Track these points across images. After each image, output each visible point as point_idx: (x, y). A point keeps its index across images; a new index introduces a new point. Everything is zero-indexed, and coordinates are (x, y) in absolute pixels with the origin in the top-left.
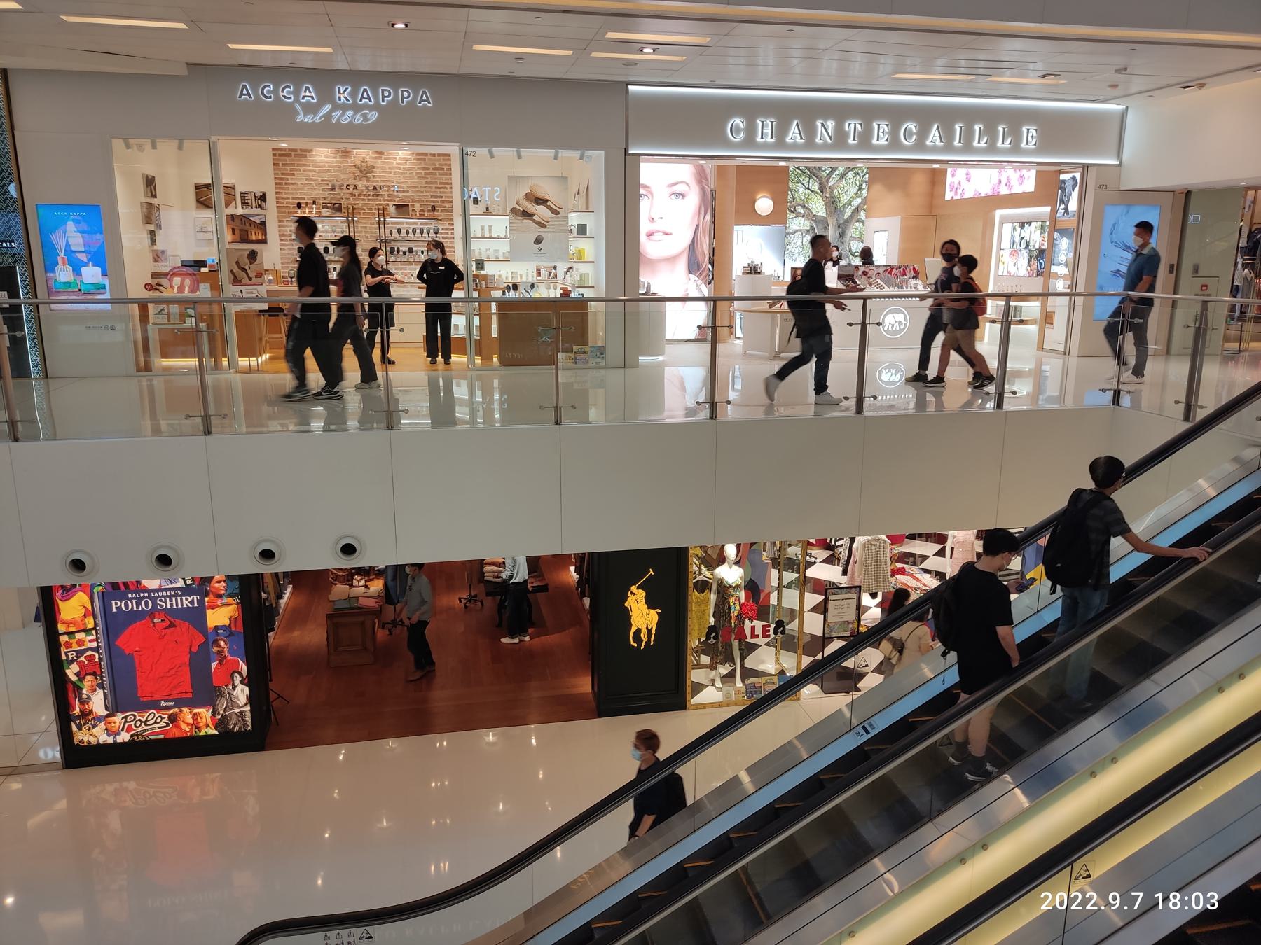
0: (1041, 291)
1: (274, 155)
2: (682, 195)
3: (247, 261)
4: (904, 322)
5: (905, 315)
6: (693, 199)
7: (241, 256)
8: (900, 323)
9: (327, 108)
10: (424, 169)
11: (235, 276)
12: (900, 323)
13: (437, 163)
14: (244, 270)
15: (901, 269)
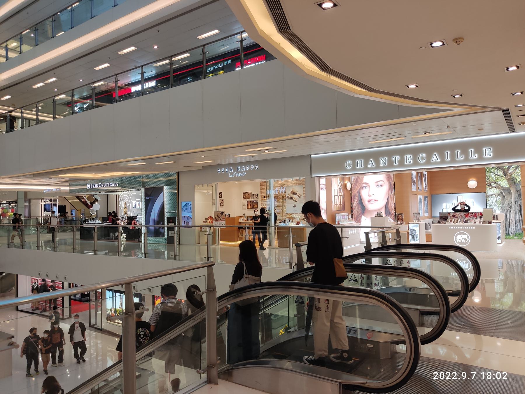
0: (370, 226)
1: (261, 183)
2: (382, 186)
3: (220, 215)
4: (467, 239)
5: (467, 236)
6: (386, 187)
7: (218, 213)
8: (465, 239)
9: (235, 173)
10: (298, 183)
11: (216, 219)
12: (465, 239)
13: (302, 181)
14: (219, 217)
15: (474, 214)
